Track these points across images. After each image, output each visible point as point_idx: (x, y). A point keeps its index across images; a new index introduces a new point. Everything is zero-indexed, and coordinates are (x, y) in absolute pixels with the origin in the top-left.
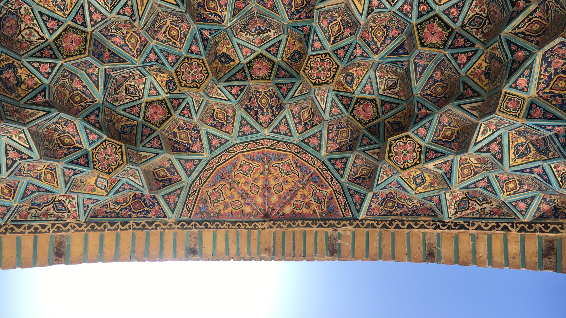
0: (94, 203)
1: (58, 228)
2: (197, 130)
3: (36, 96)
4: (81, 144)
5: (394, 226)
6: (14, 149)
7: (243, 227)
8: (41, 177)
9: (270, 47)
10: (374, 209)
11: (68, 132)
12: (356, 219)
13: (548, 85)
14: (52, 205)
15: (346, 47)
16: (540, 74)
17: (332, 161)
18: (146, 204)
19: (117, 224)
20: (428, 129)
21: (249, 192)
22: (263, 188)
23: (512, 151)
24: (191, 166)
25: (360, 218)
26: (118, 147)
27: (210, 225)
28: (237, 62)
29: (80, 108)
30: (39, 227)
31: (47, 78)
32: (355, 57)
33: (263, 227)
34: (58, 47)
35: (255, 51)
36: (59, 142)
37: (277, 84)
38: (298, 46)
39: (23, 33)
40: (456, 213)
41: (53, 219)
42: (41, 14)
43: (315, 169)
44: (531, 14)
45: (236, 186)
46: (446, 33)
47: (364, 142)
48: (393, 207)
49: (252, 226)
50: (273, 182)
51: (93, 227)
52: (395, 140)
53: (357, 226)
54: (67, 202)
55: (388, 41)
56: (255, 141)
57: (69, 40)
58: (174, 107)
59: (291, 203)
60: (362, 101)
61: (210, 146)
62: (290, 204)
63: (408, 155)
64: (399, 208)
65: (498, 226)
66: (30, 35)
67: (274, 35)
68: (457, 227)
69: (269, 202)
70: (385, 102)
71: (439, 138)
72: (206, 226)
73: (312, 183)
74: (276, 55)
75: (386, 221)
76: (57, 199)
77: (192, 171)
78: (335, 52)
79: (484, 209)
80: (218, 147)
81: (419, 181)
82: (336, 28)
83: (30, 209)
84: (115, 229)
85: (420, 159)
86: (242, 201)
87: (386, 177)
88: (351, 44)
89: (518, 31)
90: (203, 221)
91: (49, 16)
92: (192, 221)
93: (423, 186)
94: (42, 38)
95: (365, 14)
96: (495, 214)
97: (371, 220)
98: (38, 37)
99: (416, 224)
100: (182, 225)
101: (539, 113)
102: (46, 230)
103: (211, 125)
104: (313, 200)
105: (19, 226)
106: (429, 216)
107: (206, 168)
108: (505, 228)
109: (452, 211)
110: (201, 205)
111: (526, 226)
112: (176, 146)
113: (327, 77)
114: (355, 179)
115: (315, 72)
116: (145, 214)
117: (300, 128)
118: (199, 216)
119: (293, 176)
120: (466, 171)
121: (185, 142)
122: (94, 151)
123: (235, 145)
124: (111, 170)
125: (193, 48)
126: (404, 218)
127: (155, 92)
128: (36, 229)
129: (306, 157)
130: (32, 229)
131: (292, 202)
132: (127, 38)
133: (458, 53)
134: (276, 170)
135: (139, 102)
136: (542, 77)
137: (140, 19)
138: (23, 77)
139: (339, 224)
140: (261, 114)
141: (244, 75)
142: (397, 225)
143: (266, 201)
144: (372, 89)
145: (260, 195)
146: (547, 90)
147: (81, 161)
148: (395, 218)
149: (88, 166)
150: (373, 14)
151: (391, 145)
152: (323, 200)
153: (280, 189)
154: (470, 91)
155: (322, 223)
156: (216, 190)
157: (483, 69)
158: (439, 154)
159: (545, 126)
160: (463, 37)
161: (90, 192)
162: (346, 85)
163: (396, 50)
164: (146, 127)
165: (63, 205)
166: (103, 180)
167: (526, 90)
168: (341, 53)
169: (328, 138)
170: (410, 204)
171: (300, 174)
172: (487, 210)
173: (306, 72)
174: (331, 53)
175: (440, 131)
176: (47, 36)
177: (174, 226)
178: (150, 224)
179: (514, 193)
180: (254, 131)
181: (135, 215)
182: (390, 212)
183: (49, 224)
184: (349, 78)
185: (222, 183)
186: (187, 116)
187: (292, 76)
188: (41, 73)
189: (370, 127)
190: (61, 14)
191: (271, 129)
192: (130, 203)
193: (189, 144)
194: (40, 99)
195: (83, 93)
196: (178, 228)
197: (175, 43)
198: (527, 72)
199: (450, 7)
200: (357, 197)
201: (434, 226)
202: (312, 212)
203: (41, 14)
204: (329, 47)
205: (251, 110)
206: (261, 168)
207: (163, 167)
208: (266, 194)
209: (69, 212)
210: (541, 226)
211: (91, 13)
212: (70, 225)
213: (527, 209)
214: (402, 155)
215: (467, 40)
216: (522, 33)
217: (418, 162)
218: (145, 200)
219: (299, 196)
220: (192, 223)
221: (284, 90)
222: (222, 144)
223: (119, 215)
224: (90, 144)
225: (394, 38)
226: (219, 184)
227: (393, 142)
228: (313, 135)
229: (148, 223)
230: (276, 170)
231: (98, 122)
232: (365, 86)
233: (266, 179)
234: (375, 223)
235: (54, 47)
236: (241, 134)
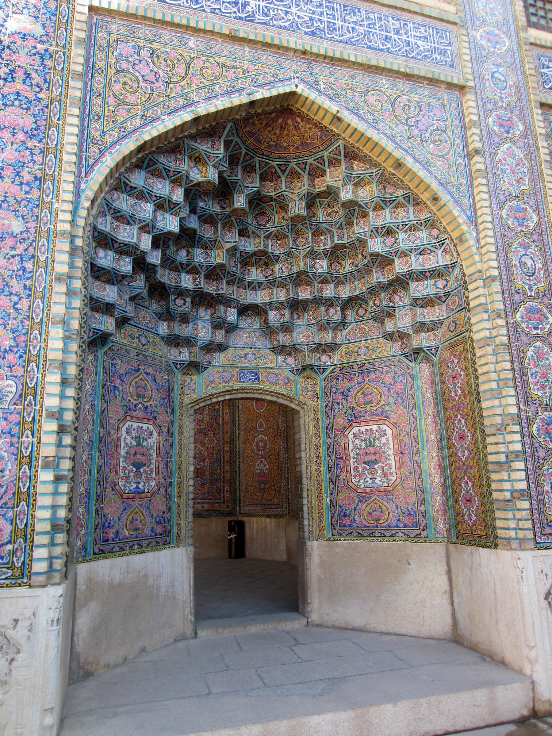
50: (278, 132)
69: (284, 119)
81: (198, 159)
219: (264, 123)
233: (281, 134)
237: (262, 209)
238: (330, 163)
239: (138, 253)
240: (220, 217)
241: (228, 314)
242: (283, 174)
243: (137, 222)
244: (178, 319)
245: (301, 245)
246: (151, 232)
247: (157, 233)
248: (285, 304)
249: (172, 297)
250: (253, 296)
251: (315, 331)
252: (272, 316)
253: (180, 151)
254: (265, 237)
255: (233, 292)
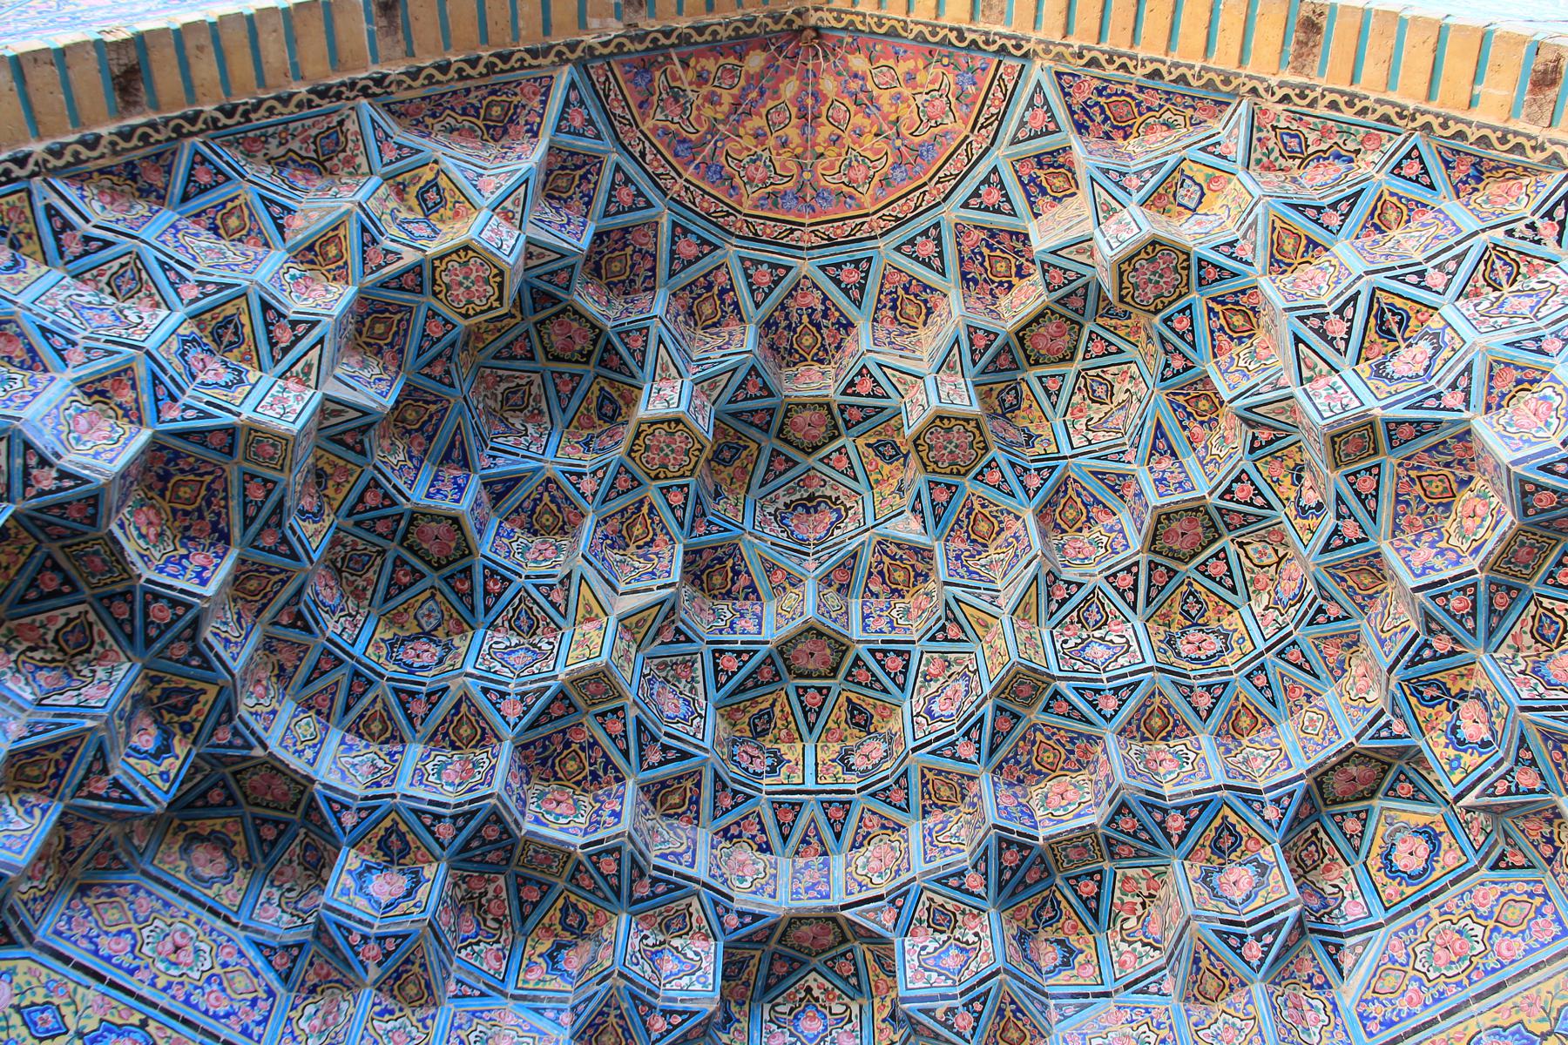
0: (1214, 145)
1: (1302, 96)
2: (968, 281)
3: (1270, 443)
4: (1210, 310)
5: (482, 63)
6: (1330, 342)
7: (868, 20)
8: (1307, 247)
9: (786, 471)
10: (535, 94)
11: (1232, 339)
12: (576, 63)
13: (209, 489)
14: (1310, 151)
15: (613, 495)
16: (226, 507)
17: (642, 204)
18: (1103, 111)
19: (1173, 77)
20: (424, 335)
21: (853, 108)
22: (815, 118)
23: (247, 330)
24: (989, 194)
25: (567, 68)
26: (1128, 299)
27: (952, 36)
28: (861, 442)
29: (1200, 386)
30: (1342, 106)
31: (1243, 471)
32: (594, 473)
33: (820, 14)
34: (1214, 526)
35: (821, 460)
36: (1254, 320)
37: (771, 395)
38: (724, 475)
39: (1275, 559)
40: (341, 123)
41: (1312, 120)
42: (1233, 590)
43: (686, 176)
44: (265, 606)
45: (885, 127)
46: (412, 538)
47: (565, 275)
48: (489, 106)
49: (846, 18)
50: (792, 133)
51: (1227, 82)
52: (491, 308)
53: (572, 47)
54: (1276, 154)
55: (528, 504)
56: (832, 242)
57: (1188, 540)
58: (1010, 351)
59: (747, 81)
60: (577, 356)
61: (939, 239)
62: (749, 77)
63: (460, 278)
64: (473, 106)
65: (246, 114)
66: (1262, 554)
67: (777, 497)
68: (334, 90)
69: (803, 79)
70: (527, 359)
71: (398, 317)
72: (961, 38)
73: (693, 137)
74: (776, 453)
75: (502, 71)
76: (1298, 161)
77: (986, 181)
78: (637, 483)
79: (281, 144)
80: (921, 234)
81: (432, 195)
82: (638, 530)
83: (1357, 152)
84: (1177, 65)
85: (434, 269)
86: (870, 86)
87: (508, 204)
88: (604, 502)
89: (282, 576)
90: (968, 48)
91: (1220, 583)
92: (996, 53)
93: (422, 183)
94: (1241, 545)
95: (575, 579)
96: (255, 140)
97: (539, 66)
98: (1248, 548)
99: (430, 77)
100: (1018, 47)
101: (215, 440)
102: (1329, 97)
103: (933, 290)
104: (690, 93)
105: (1386, 119)
106: (402, 102)
107: (953, 182)
108: (230, 113)
109: (351, 126)
110: (971, 89)
111: (187, 128)
112: (1019, 246)
113: (652, 434)
114: (585, 164)
115: (679, 444)
116: (1105, 88)
117: (721, 279)
118: (979, 64)
119: (740, 152)
120: (332, 251)
121: (998, 253)
122: (1184, 290)
123: (882, 235)
124: (1150, 249)
125: (944, 497)
126: (460, 85)
127: (1049, 383)
128: (1350, 104)
129: (708, 204)
130: (1359, 106)
131: (743, 82)
132: (1084, 518)
133: (385, 507)
134: (783, 166)
135: (1088, 364)
136: (223, 503)
137: (1036, 578)
138: (1287, 481)
139: (620, 46)
140: (814, 310)
141: (846, 415)
142: (474, 67)
143: (810, 79)
144: (556, 385)
145: (825, 97)
146: (209, 478)
147: (1213, 274)
148: (481, 82)
149: (1200, 260)
150: (561, 576)
151: (500, 299)
152: (664, 96)
153: (774, 117)
154: (350, 441)
155: (663, 41)
156: (933, 123)
157: (330, 483)
158: (393, 285)
159: (198, 418)
160: (380, 535)
161: (1218, 173)
162: (615, 395)
163: (509, 489)
164: (1076, 311)
165: (1285, 145)
166: (1185, 202)
167: (247, 478)
168: (623, 483)
169: (654, 257)
170: (449, 120)
171: (723, 159)
172: (274, 142)
173: (697, 446)
174: (647, 480)
175: (396, 333)
176: (1232, 549)
177: (1039, 49)
178: (1094, 62)
179: (224, 204)
180: (832, 271)
181: (1131, 89)
182: (494, 93)
183: (1321, 110)
184: (608, 409)
185: (917, 140)
186: (980, 333)
187: (736, 415)
188: (1253, 484)
189: (554, 304)
190: (1196, 586)
191: (792, 274)
192: (1140, 120)
193: (989, 246)
194: (1264, 435)
195: (1190, 414)
196: (1028, 41)
197: (983, 506)
198: (251, 511)
199: (412, 584)
200: (578, 122)
201: (387, 82)
202: (692, 62)
203: (1233, 590)
204: (653, 493)
205: (838, 322)
206: (820, 171)
207: (1055, 198)
208: (810, 101)
209: (1274, 128)
210: (157, 137)
211: (1135, 589)
212: (1276, 98)
213: (193, 168)
214: (472, 277)
215: (371, 530)
216: (274, 574)
217: (437, 263)
218: (1104, 122)
219: (727, 99)
220: (995, 47)
221: (755, 385)
222: (912, 242)
223: (1164, 97)
224: (1189, 307)
225: (516, 511)
226: (925, 137)
227: (496, 304)
228: (690, 263)
229: (1099, 66)
230: (783, 166)
231: (1166, 353)
232: (573, 391)
234: (529, 60)
235: (1222, 526)
236: (864, 265)
237: (802, 482)
238: (1034, 189)
239: (47, 479)
240: (587, 485)
241: (669, 965)
242: (858, 304)
243: (75, 356)
244: (374, 972)
245: (999, 575)
246: (148, 414)
247: (175, 418)
248: (973, 881)
249: (350, 860)
250: (807, 880)
251: (1168, 1002)
252: (913, 960)
253: (348, 162)
254: (826, 580)
255: (685, 847)
